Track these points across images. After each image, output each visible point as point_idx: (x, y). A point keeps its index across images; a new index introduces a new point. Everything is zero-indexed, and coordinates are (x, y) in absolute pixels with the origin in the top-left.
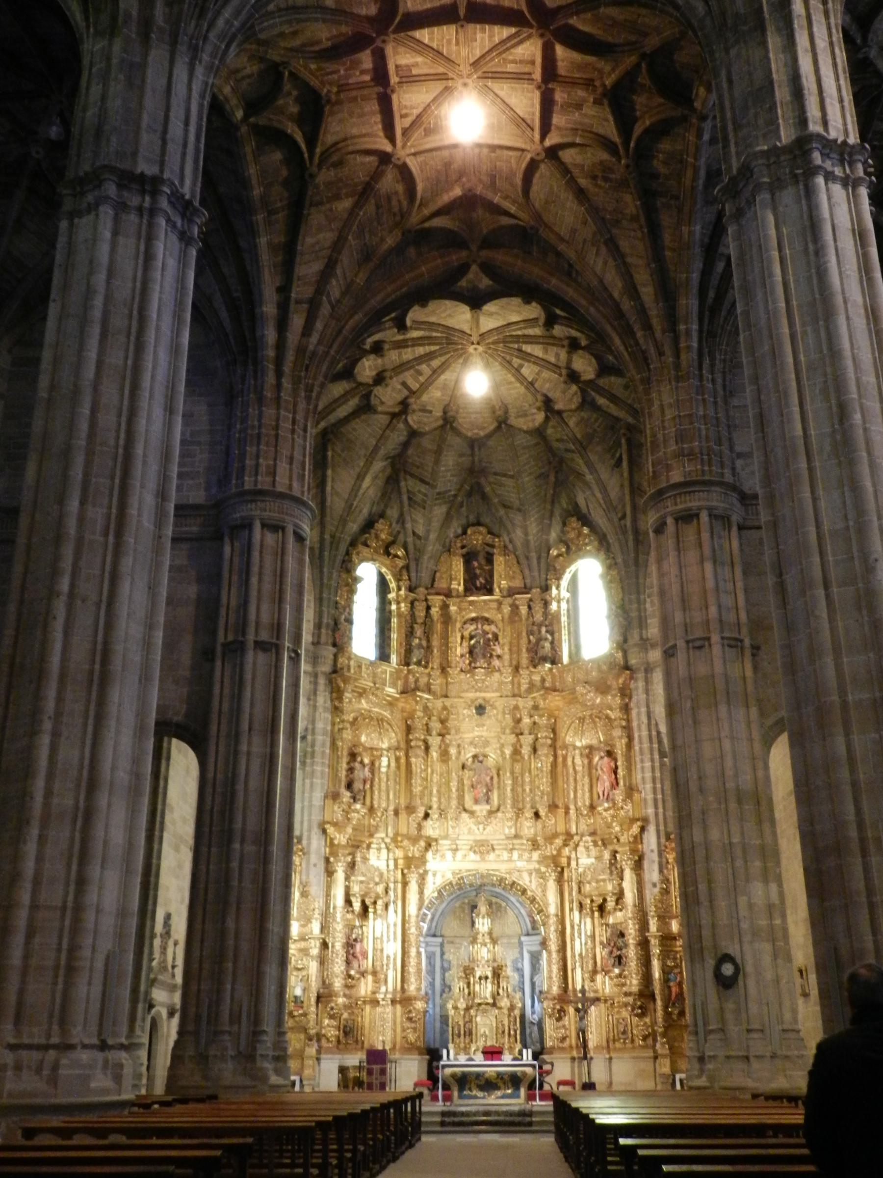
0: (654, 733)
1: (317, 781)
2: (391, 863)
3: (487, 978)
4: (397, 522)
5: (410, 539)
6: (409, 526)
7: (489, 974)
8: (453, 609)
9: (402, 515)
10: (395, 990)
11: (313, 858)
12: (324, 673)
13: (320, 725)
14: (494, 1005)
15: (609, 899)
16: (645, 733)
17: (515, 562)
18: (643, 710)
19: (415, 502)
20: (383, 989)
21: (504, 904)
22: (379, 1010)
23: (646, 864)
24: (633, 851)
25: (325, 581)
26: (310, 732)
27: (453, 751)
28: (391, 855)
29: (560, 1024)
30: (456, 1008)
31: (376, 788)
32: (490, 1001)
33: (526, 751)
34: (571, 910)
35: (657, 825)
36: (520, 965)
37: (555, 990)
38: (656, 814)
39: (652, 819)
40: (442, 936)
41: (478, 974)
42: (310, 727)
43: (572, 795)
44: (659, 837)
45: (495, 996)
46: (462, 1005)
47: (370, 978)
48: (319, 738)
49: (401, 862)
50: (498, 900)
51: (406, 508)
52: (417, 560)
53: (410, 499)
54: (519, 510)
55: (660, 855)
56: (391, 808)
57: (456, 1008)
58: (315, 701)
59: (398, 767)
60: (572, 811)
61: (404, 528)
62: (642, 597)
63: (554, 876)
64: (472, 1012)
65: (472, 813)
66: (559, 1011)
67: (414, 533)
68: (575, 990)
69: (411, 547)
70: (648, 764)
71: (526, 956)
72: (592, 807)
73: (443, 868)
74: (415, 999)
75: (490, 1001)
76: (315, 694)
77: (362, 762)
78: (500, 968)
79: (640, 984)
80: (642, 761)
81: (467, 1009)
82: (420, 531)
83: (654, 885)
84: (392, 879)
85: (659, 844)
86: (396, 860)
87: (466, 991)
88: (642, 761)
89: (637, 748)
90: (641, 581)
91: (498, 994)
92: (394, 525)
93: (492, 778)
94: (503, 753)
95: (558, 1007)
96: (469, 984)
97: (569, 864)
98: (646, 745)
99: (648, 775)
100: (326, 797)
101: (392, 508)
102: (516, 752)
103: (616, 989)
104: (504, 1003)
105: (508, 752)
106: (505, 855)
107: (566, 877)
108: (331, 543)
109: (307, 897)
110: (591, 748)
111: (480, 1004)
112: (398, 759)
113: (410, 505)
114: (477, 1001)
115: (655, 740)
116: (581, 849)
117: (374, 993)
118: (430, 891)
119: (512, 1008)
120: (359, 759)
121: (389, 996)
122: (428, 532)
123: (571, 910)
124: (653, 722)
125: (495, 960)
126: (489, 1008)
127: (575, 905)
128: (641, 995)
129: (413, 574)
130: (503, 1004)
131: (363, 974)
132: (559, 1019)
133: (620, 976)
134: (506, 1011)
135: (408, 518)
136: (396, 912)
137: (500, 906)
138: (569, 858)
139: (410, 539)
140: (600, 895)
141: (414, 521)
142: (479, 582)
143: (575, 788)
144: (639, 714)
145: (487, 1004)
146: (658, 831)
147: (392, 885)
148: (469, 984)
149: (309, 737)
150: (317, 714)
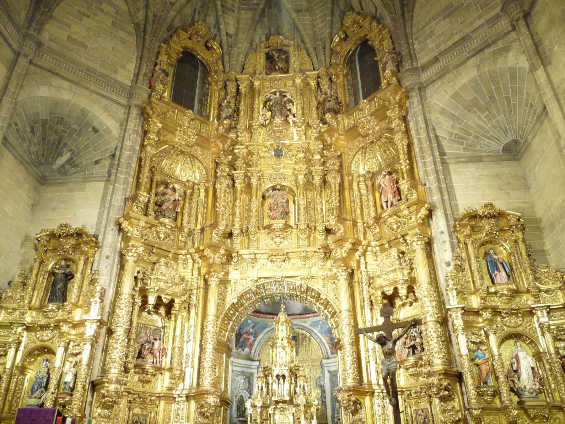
0: (432, 136)
1: (120, 186)
2: (196, 273)
3: (284, 377)
4: (214, 28)
5: (224, 38)
6: (222, 27)
7: (287, 373)
8: (257, 83)
9: (217, 21)
10: (191, 386)
11: (106, 251)
12: (136, 106)
13: (128, 143)
14: (291, 402)
15: (399, 287)
16: (423, 135)
17: (306, 55)
18: (420, 118)
19: (227, 8)
20: (181, 386)
21: (308, 335)
22: (174, 406)
23: (436, 247)
24: (423, 233)
25: (147, 45)
26: (119, 149)
27: (254, 181)
28: (196, 265)
29: (357, 417)
30: (254, 406)
31: (186, 211)
32: (287, 398)
33: (317, 180)
34: (362, 308)
35: (445, 211)
36: (322, 383)
37: (350, 382)
38: (443, 201)
39: (438, 204)
40: (260, 361)
41: (275, 374)
42: (120, 145)
43: (359, 212)
44: (447, 221)
45: (293, 394)
46: (259, 404)
47: (167, 375)
48: (126, 153)
49: (204, 271)
50: (304, 332)
51: (220, 13)
52: (229, 54)
53: (223, 6)
54: (307, 11)
55: (451, 236)
56: (199, 227)
57: (254, 406)
58: (126, 125)
59: (207, 196)
60: (360, 225)
61: (219, 30)
62: (410, 41)
63: (343, 276)
64: (270, 411)
65: (268, 227)
66: (355, 403)
67: (227, 33)
68: (370, 383)
69: (225, 45)
70: (429, 159)
71: (327, 375)
72: (378, 219)
73: (242, 279)
74: (208, 393)
75: (287, 398)
76: (127, 120)
77: (174, 190)
78: (297, 368)
79: (444, 364)
80: (423, 157)
81: (265, 407)
82: (232, 31)
83: (448, 264)
84: (195, 285)
85: (448, 226)
86: (199, 269)
87: (265, 390)
88: (423, 157)
89: (417, 150)
90: (409, 31)
91: (296, 393)
92: (212, 30)
93: (287, 202)
94: (296, 181)
95: (353, 399)
96: (267, 384)
97: (359, 267)
98: (425, 145)
99: (430, 168)
100: (126, 200)
101: (210, 16)
102: (309, 184)
103: (412, 380)
104: (300, 400)
105: (301, 177)
106: (299, 263)
107: (356, 279)
108: (154, 21)
109: (93, 285)
110: (373, 176)
111: (277, 402)
112: (207, 191)
113: (223, 12)
114: (274, 399)
115: (433, 140)
116: (369, 254)
117: (170, 389)
118: (231, 298)
119: (308, 405)
120: (171, 186)
121: (185, 392)
122: (237, 34)
123: (362, 308)
124: (430, 127)
125: (292, 362)
126: (285, 406)
127: (367, 303)
128: (446, 374)
129: (227, 64)
130: (299, 401)
131: (159, 370)
132: (355, 412)
133: (415, 365)
134: (302, 408)
135: (222, 21)
136: (196, 314)
137: (306, 336)
138: (358, 262)
139: (224, 38)
140: (391, 284)
141: (227, 24)
142: (276, 61)
143: (362, 206)
144: (416, 122)
145: (284, 402)
146: (446, 215)
147: (195, 292)
148: (267, 384)
149: (118, 153)
150: (127, 134)
